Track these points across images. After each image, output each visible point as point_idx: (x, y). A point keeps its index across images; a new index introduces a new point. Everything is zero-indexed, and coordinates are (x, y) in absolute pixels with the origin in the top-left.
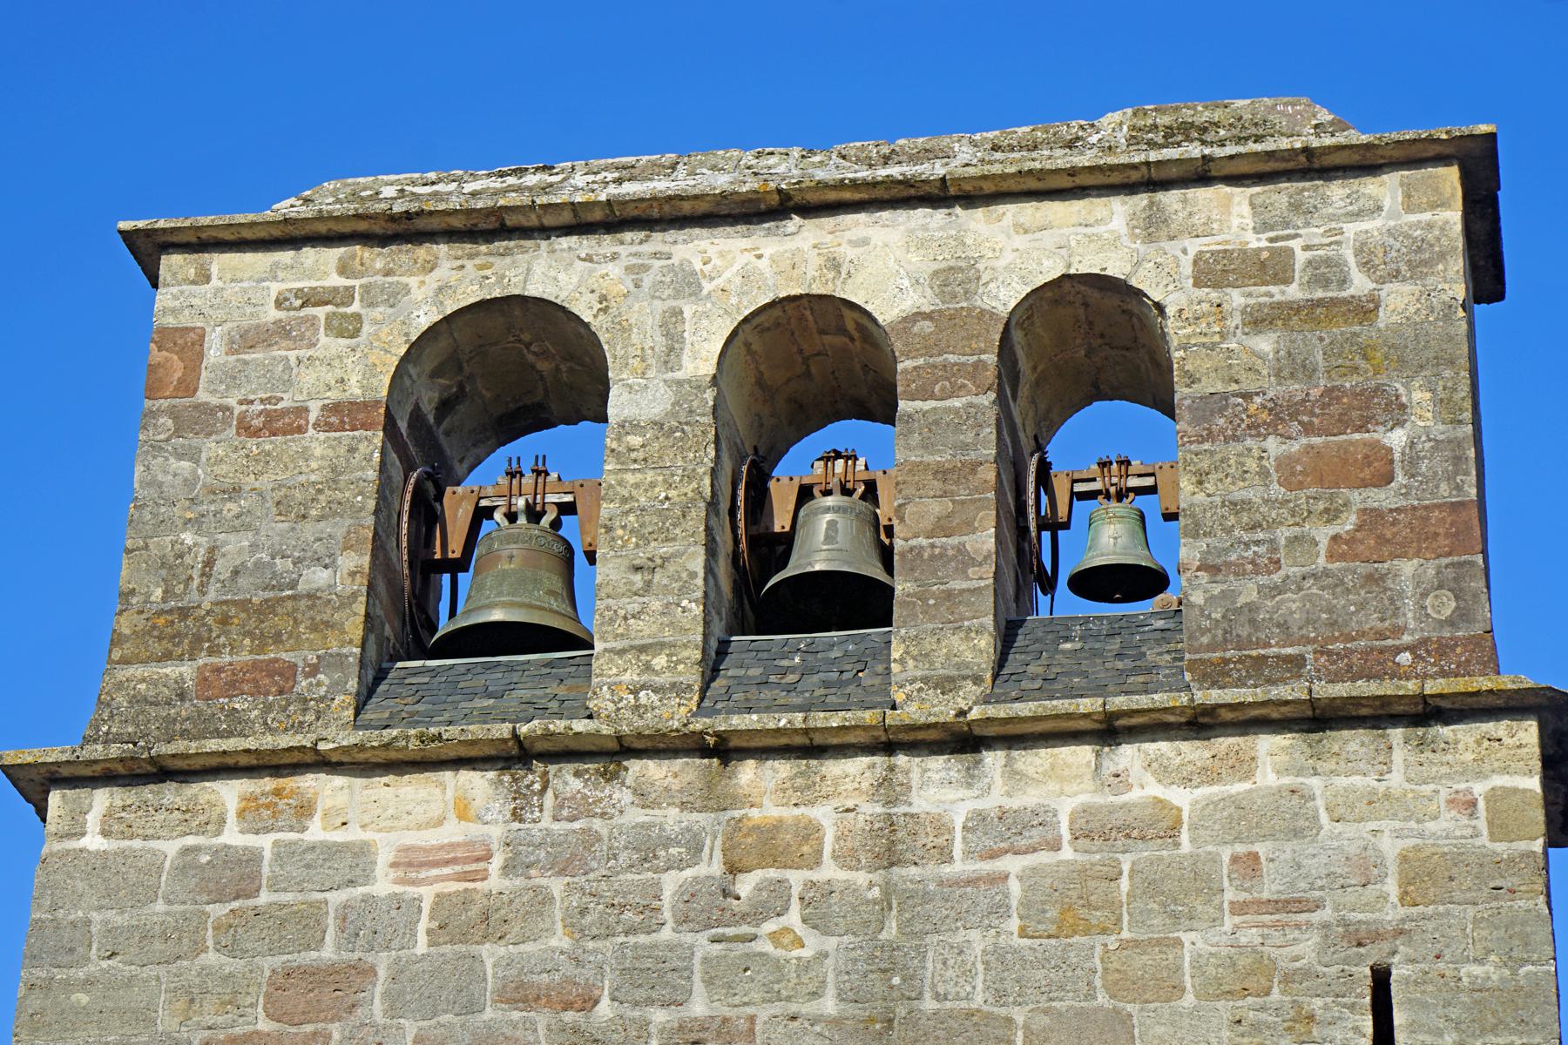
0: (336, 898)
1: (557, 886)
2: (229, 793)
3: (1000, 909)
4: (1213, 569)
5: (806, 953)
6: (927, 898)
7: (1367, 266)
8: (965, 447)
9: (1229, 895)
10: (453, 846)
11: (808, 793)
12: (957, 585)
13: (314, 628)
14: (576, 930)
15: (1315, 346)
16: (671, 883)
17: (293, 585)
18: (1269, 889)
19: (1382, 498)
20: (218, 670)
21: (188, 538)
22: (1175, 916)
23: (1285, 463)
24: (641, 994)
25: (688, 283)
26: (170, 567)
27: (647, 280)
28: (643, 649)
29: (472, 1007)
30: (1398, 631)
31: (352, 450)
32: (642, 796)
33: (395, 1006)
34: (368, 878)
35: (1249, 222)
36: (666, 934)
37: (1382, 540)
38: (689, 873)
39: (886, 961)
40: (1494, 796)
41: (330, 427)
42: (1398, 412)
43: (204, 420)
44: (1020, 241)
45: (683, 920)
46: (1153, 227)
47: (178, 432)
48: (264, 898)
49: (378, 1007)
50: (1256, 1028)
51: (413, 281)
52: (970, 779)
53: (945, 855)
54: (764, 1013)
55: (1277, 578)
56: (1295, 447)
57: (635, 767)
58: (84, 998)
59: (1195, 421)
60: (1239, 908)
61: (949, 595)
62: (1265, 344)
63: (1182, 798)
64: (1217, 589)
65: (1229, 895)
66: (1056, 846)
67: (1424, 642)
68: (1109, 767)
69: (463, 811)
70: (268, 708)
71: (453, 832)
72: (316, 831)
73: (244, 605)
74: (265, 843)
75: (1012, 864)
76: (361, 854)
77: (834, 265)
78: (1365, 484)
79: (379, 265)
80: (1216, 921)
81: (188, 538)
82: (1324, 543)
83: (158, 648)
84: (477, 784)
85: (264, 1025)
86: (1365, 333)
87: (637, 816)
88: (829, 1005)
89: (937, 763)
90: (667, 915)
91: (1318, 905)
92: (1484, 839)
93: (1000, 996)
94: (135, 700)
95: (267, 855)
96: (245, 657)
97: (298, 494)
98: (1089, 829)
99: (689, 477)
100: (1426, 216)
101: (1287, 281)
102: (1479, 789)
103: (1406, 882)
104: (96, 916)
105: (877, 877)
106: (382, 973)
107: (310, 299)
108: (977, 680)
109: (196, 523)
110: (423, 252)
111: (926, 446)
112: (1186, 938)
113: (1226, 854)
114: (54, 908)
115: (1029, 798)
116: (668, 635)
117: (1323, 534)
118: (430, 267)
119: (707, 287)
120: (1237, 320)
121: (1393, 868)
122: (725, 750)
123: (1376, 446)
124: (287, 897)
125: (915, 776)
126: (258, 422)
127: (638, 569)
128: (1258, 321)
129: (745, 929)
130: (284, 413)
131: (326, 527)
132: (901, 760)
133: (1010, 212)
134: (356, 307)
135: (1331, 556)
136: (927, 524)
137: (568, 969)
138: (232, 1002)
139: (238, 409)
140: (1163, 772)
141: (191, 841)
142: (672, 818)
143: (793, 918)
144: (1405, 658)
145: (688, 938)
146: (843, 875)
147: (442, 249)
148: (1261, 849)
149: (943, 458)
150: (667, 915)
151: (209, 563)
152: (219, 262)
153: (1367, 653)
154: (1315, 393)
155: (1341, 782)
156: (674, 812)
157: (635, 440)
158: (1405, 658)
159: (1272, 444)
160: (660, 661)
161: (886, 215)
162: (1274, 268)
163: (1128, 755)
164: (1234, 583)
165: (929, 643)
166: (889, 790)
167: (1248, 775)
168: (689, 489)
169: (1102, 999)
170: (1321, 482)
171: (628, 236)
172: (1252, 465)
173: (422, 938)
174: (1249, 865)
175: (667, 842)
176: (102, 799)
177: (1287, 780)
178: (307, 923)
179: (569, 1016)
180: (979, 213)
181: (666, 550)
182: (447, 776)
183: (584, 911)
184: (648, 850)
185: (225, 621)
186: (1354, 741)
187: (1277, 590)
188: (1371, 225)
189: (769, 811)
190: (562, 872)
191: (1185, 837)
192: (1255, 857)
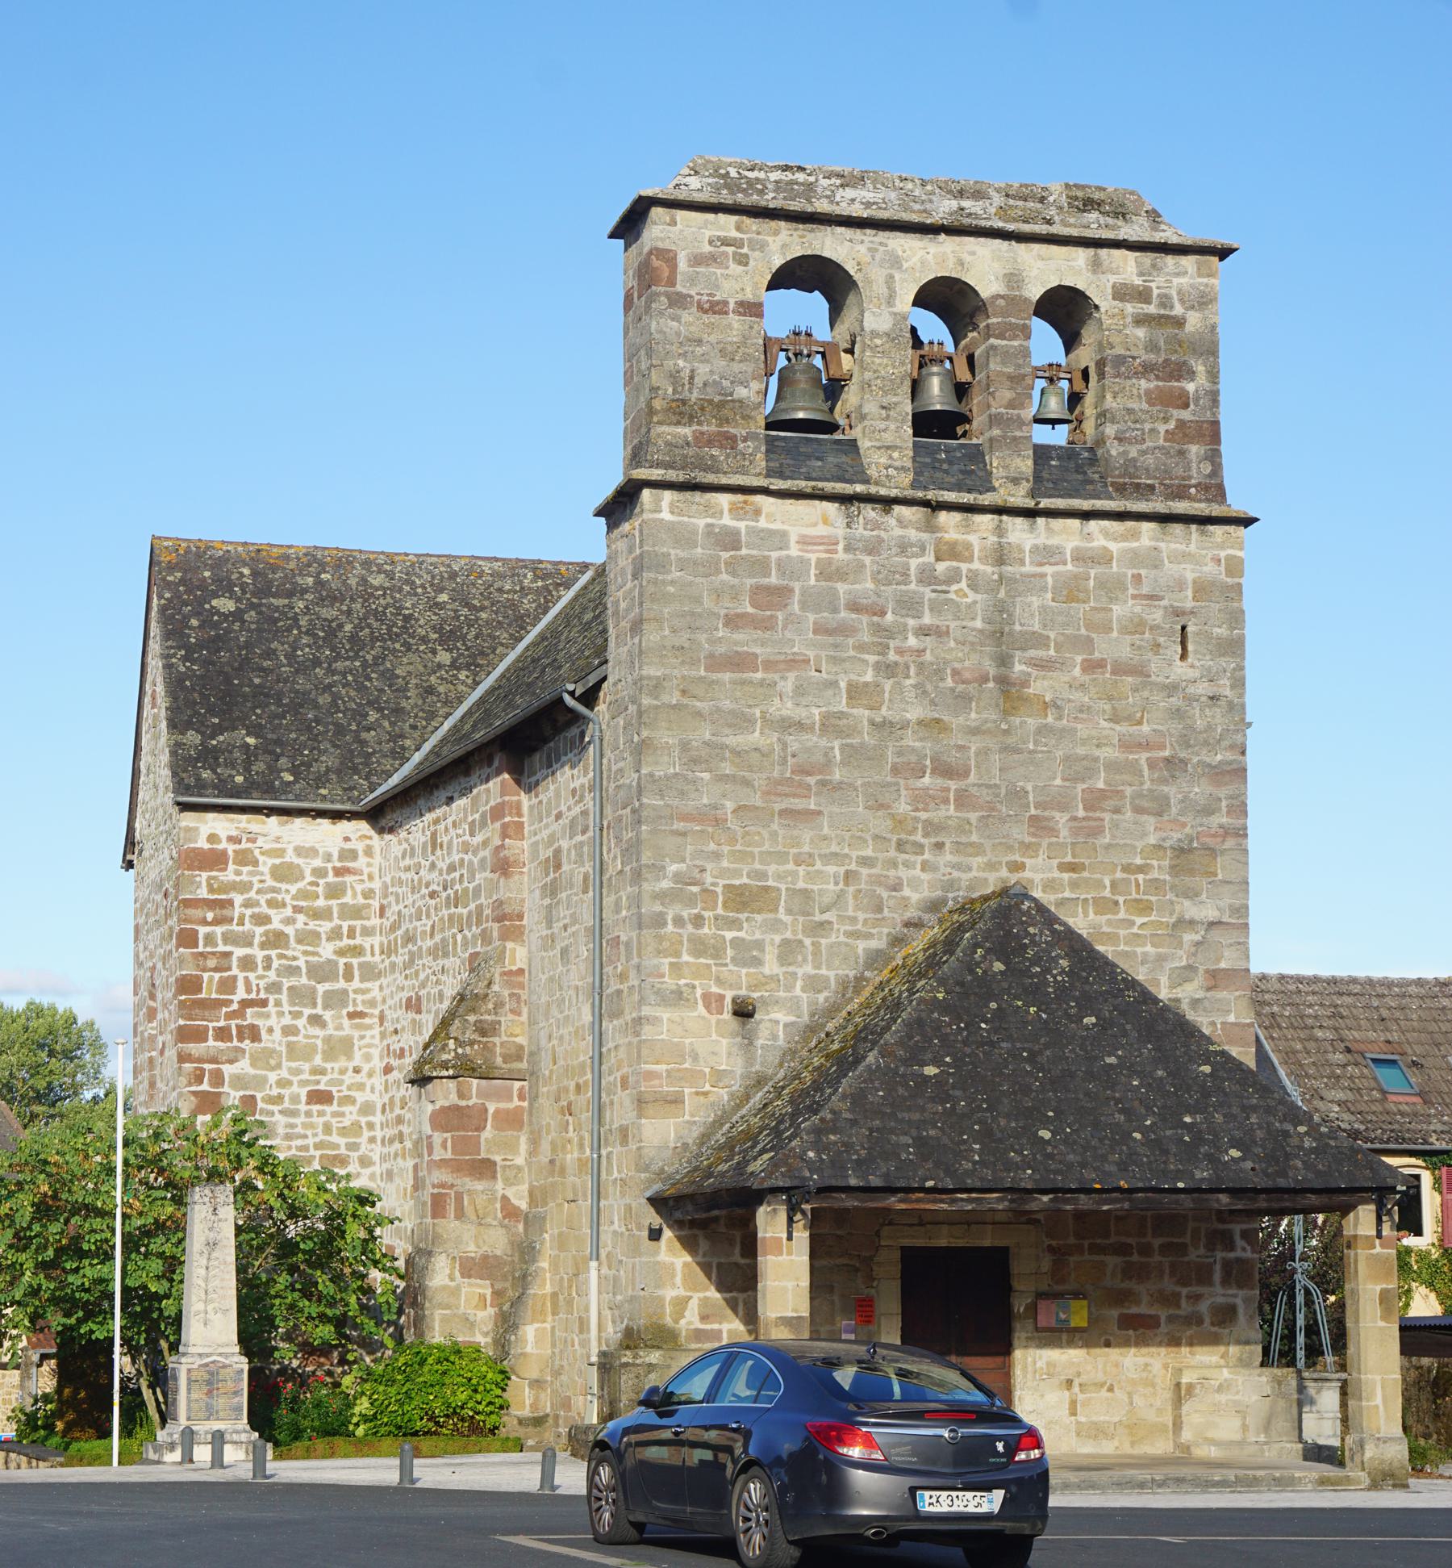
0: (774, 555)
1: (867, 560)
2: (724, 499)
3: (1044, 589)
4: (1120, 439)
5: (969, 600)
6: (1016, 581)
7: (1182, 301)
8: (1019, 366)
9: (1131, 591)
10: (823, 537)
11: (967, 528)
12: (1018, 434)
13: (743, 418)
14: (874, 579)
15: (1161, 335)
16: (914, 563)
17: (731, 394)
18: (1145, 590)
19: (1186, 415)
20: (702, 433)
21: (681, 363)
22: (1111, 598)
23: (1148, 392)
24: (904, 612)
25: (895, 262)
26: (674, 376)
27: (878, 256)
28: (888, 448)
29: (836, 611)
30: (1190, 478)
31: (751, 328)
32: (901, 522)
33: (804, 606)
34: (787, 548)
35: (1135, 271)
36: (913, 586)
37: (1185, 435)
38: (921, 560)
39: (1001, 608)
40: (1229, 558)
41: (740, 314)
42: (1191, 375)
43: (679, 301)
44: (1040, 264)
45: (920, 581)
46: (1096, 265)
47: (670, 306)
48: (744, 551)
49: (796, 607)
50: (1139, 648)
51: (770, 239)
52: (1032, 529)
53: (1022, 562)
54: (953, 625)
55: (1144, 447)
56: (1152, 385)
57: (898, 509)
58: (671, 589)
59: (1114, 367)
60: (1134, 597)
61: (1015, 439)
62: (1141, 333)
63: (1113, 547)
64: (1121, 449)
65: (1131, 591)
66: (1065, 563)
67: (1200, 484)
68: (1086, 530)
69: (826, 521)
70: (728, 456)
71: (821, 530)
72: (763, 523)
73: (710, 402)
74: (742, 525)
75: (1049, 570)
76: (784, 535)
77: (961, 263)
78: (1178, 407)
79: (754, 228)
80: (1126, 602)
81: (681, 363)
82: (1162, 433)
83: (674, 418)
84: (831, 508)
85: (750, 610)
86: (1181, 335)
87: (898, 532)
88: (978, 624)
89: (1019, 520)
90: (913, 578)
91: (1161, 598)
92: (1223, 576)
93: (1045, 626)
94: (668, 444)
95: (743, 531)
96: (713, 428)
97: (729, 348)
98: (1080, 557)
99: (902, 363)
100: (1205, 280)
101: (1150, 303)
102: (1223, 554)
103: (1195, 592)
104: (672, 552)
105: (996, 569)
106: (797, 591)
107: (726, 242)
108: (1028, 481)
109: (684, 355)
110: (774, 224)
111: (1003, 363)
112: (1114, 607)
113: (1130, 573)
114: (654, 545)
115: (1054, 541)
116: (898, 443)
117: (1162, 428)
118: (776, 233)
119: (905, 265)
120: (1129, 320)
121: (1190, 586)
122: (936, 507)
123: (1183, 389)
124: (754, 552)
125: (1010, 526)
126: (707, 306)
127: (884, 408)
128: (1140, 320)
129: (944, 588)
130: (718, 303)
131: (743, 367)
132: (1005, 518)
133: (1036, 247)
134: (745, 250)
135: (1165, 440)
136: (1005, 402)
137: (874, 598)
138: (735, 598)
139: (697, 298)
140: (1106, 534)
141: (709, 520)
142: (913, 534)
143: (963, 584)
144: (1193, 490)
145: (922, 589)
146: (982, 567)
147: (782, 224)
148: (1143, 572)
149: (1010, 370)
150: (913, 578)
151: (692, 378)
152: (681, 215)
153: (1179, 486)
154: (1161, 360)
155: (1173, 546)
156: (913, 532)
157: (878, 342)
158: (1193, 490)
159: (1143, 382)
160: (896, 455)
161: (982, 240)
162: (1144, 296)
163: (1094, 525)
164: (1128, 447)
165: (1008, 461)
166: (1000, 531)
167: (1138, 540)
168: (902, 369)
169: (1083, 631)
170: (1162, 404)
171: (868, 231)
172: (1135, 392)
173: (813, 578)
174: (1138, 578)
175: (912, 545)
176: (668, 496)
177: (1153, 543)
178: (762, 566)
179: (875, 619)
180: (1023, 246)
181: (894, 399)
182: (817, 502)
183: (879, 572)
184: (903, 547)
185: (702, 409)
186: (1177, 529)
187: (1144, 453)
188: (1184, 280)
189: (952, 535)
190: (870, 554)
191: (1114, 564)
192: (1140, 575)
